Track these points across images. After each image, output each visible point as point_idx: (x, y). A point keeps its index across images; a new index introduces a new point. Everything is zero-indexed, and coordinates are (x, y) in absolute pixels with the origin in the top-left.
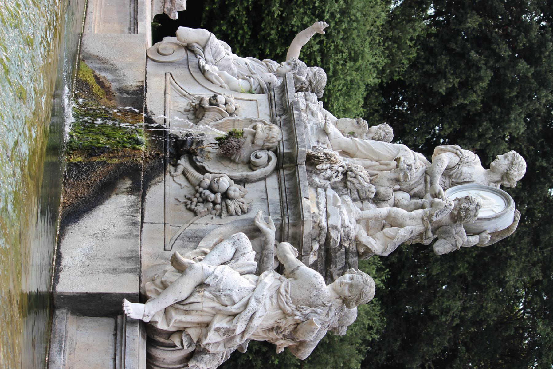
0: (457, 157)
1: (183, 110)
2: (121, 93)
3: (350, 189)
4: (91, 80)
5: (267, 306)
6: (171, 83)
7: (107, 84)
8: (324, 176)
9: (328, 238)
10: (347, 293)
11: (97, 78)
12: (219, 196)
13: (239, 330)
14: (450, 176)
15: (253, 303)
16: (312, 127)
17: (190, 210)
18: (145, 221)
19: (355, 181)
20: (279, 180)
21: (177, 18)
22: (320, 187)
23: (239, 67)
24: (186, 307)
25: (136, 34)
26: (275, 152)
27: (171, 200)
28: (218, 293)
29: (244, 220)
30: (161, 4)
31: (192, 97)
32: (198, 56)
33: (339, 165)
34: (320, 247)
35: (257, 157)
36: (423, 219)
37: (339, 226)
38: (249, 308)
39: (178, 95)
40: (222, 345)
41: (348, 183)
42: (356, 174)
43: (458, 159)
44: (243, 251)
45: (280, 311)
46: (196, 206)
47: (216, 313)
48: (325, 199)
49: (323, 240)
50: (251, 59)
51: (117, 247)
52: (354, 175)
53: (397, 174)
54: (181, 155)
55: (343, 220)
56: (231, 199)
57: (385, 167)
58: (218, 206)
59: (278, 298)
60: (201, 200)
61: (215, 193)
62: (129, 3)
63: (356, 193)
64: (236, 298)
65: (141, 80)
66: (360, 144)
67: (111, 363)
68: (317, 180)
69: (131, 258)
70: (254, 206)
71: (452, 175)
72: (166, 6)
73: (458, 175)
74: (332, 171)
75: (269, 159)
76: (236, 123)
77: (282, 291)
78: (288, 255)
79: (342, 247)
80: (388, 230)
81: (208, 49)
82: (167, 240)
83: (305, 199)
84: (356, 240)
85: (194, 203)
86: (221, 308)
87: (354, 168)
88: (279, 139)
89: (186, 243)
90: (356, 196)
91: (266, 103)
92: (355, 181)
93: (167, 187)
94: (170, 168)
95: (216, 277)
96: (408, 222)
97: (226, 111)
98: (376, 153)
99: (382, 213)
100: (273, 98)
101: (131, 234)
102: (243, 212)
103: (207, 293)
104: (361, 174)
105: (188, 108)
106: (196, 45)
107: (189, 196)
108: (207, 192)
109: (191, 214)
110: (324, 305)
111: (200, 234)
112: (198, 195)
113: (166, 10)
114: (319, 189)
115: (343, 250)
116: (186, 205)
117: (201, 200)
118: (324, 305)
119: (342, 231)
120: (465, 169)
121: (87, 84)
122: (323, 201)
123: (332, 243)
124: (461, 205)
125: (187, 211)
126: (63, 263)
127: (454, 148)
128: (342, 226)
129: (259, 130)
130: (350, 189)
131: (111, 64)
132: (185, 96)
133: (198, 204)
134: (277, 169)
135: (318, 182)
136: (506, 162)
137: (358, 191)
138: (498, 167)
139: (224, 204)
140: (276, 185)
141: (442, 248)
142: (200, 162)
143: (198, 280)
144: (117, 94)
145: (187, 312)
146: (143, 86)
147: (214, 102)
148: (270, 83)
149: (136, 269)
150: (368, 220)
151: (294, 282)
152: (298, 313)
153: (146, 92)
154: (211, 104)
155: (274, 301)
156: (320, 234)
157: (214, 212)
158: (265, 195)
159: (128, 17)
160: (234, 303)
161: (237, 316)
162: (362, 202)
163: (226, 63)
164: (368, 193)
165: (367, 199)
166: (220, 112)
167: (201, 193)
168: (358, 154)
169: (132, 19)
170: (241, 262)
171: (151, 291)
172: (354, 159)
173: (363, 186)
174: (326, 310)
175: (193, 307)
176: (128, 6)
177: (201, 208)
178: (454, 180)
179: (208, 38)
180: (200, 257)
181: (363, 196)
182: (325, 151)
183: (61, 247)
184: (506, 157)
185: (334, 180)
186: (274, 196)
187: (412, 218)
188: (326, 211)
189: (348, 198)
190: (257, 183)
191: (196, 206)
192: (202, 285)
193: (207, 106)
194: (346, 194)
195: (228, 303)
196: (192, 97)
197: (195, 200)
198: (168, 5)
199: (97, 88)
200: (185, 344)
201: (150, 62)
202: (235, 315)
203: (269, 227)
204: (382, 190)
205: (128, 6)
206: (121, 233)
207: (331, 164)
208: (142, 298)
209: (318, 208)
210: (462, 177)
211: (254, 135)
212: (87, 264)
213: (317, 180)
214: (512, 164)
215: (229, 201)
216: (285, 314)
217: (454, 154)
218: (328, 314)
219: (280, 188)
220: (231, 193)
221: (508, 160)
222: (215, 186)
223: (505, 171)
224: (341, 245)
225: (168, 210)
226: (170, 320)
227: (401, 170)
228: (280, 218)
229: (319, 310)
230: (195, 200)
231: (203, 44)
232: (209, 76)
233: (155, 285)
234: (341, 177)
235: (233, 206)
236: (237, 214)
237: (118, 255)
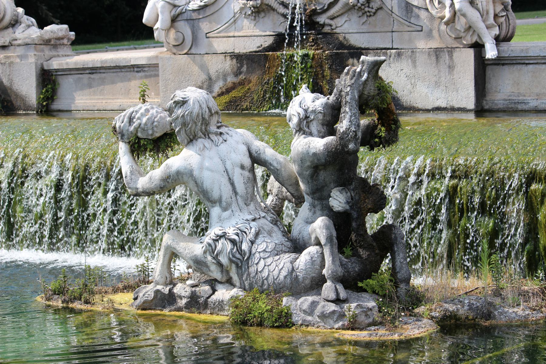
2: (240, 73)
4: (226, 98)
6: (218, 33)
7: (230, 85)
11: (221, 94)
17: (375, 13)
18: (391, 47)
21: (73, 33)
24: (485, 14)
25: (160, 66)
27: (365, 28)
30: (65, 48)
32: (184, 11)
39: (234, 27)
46: (372, 8)
51: (425, 67)
54: (313, 21)
62: (99, 75)
65: (224, 58)
67: (531, 66)
69: (437, 55)
72: (66, 43)
85: (370, 10)
89: (414, 14)
93: (350, 31)
94: (327, 29)
101: (411, 57)
105: (253, 18)
107: (360, 14)
109: (380, 12)
111: (403, 5)
112: (363, 7)
113: (69, 43)
116: (370, 16)
117: (367, 5)
121: (230, 102)
126: (443, 105)
131: (203, 83)
133: (371, 6)
142: (324, 6)
144: (242, 77)
145: (488, 13)
146: (231, 56)
149: (448, 52)
153: (233, 52)
159: (119, 74)
167: (362, 5)
169: (123, 70)
171: (472, 40)
175: (485, 8)
176: (103, 75)
183: (427, 108)
191: (372, 8)
197: (367, 9)
198: (65, 41)
199: (234, 94)
201: (193, 51)
205: (103, 75)
206: (410, 64)
212: (445, 88)
225: (378, 30)
226: (493, 25)
230: (367, 9)
231: (171, 7)
237: (434, 65)
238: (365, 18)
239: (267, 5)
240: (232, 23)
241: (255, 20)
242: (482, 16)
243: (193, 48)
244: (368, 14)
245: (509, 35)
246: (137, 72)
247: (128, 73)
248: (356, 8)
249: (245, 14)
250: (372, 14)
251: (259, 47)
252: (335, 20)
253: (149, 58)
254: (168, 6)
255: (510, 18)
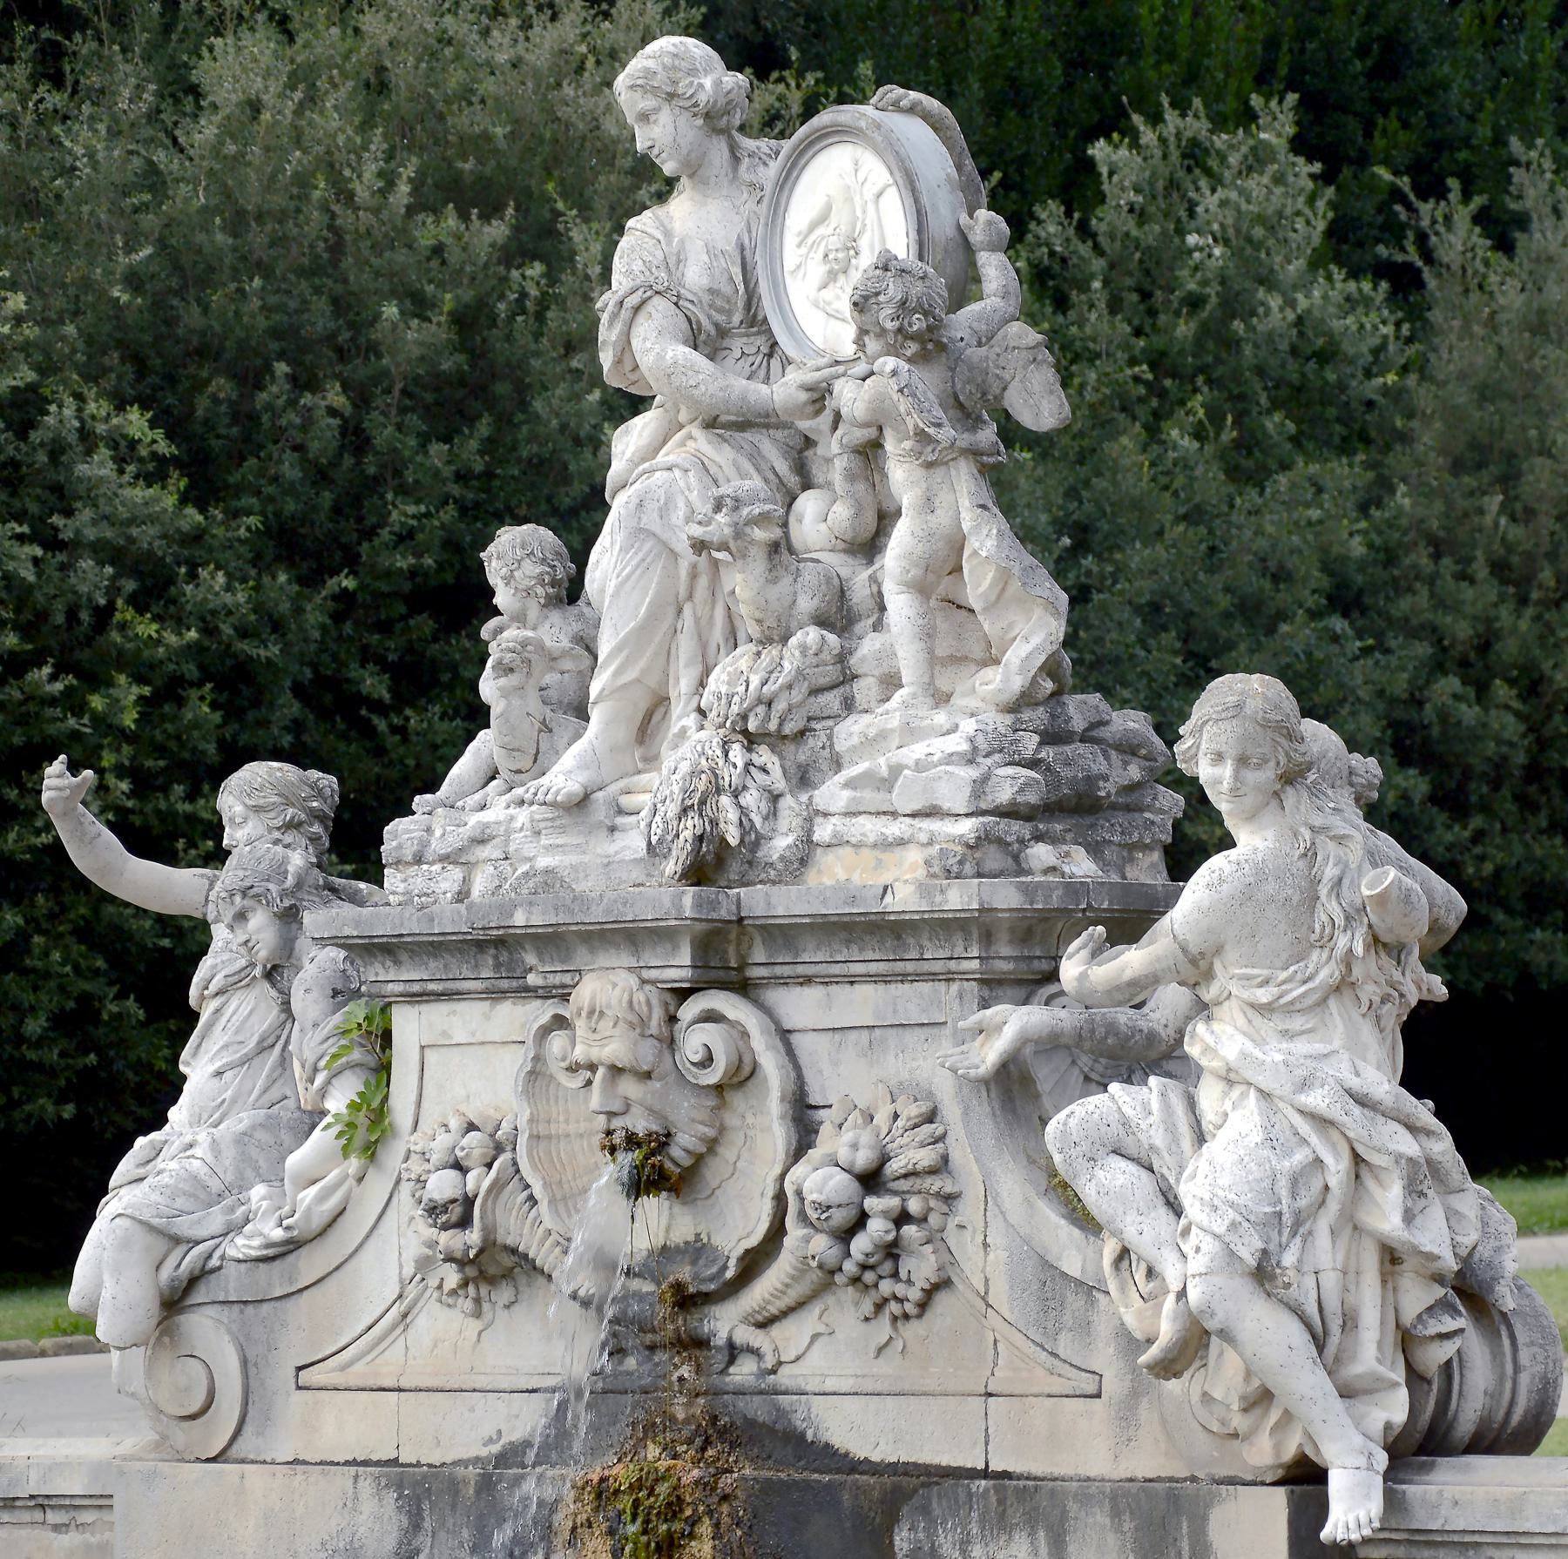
0: (649, 307)
1: (474, 1326)
3: (809, 719)
5: (1320, 1048)
6: (343, 1368)
8: (766, 818)
9: (1009, 812)
10: (1268, 774)
12: (871, 1203)
13: (1408, 1145)
14: (722, 332)
15: (1316, 1099)
16: (551, 849)
17: (923, 1306)
18: (981, 1466)
19: (780, 706)
20: (784, 982)
22: (809, 832)
23: (234, 1101)
25: (115, 1502)
26: (683, 995)
27: (887, 1370)
28: (1287, 1219)
29: (966, 1113)
31: (412, 1292)
32: (215, 1262)
33: (721, 762)
34: (1039, 838)
35: (708, 1061)
36: (929, 465)
37: (972, 773)
38: (1336, 1113)
39: (401, 1340)
40: (1457, 1202)
41: (789, 729)
42: (759, 701)
43: (657, 300)
44: (1117, 1128)
45: (1332, 1003)
46: (909, 1282)
47: (1351, 1226)
48: (861, 819)
49: (1016, 829)
50: (195, 1054)
52: (761, 709)
53: (753, 551)
55: (949, 759)
56: (884, 1159)
57: (703, 582)
58: (914, 1206)
59: (1290, 1009)
60: (887, 1267)
61: (862, 1219)
63: (823, 699)
64: (1300, 1157)
66: (617, 674)
68: (781, 844)
70: (905, 1076)
71: (717, 325)
73: (719, 303)
74: (745, 788)
75: (711, 1017)
76: (542, 1129)
77: (1263, 995)
78: (1128, 975)
79: (1040, 761)
80: (977, 586)
81: (183, 1226)
82: (1058, 1386)
83: (888, 898)
84: (1014, 708)
85: (900, 1289)
86: (1333, 1206)
87: (735, 709)
88: (633, 981)
89: (1068, 1319)
90: (832, 700)
91: (436, 1015)
92: (780, 706)
93: (830, 1385)
95: (1234, 1226)
96: (942, 518)
97: (489, 1166)
98: (652, 617)
99: (911, 612)
100: (416, 988)
102: (931, 1117)
103: (1289, 1259)
104: (755, 681)
105: (468, 1305)
106: (166, 1273)
107: (867, 1307)
108: (861, 1244)
109: (942, 1300)
110: (1310, 854)
112: (869, 1277)
114: (816, 838)
115: (1048, 753)
116: (906, 1317)
118: (1310, 854)
119: (989, 761)
120: (695, 276)
122: (869, 827)
123: (1032, 798)
124: (884, 331)
125: (929, 1315)
127: (614, 317)
128: (971, 762)
129: (596, 1054)
130: (809, 719)
132: (405, 1316)
133: (903, 1274)
134: (743, 987)
135: (790, 840)
136: (665, 117)
137: (815, 691)
138: (684, 151)
139: (903, 1185)
140: (814, 993)
141: (1040, 403)
142: (725, 1268)
143: (1243, 1289)
145: (1350, 1322)
147: (456, 1212)
148: (335, 993)
150: (934, 662)
151: (1231, 954)
152: (1342, 942)
153: (394, 1462)
154: (464, 1222)
155: (1297, 1023)
156: (1001, 842)
157: (934, 1220)
158: (853, 1035)
160: (1318, 1162)
161: (1361, 1150)
162: (855, 677)
163: (229, 1154)
164: (825, 656)
165: (842, 658)
166: (497, 1187)
167: (864, 1267)
168: (652, 681)
170: (1159, 1139)
171: (1277, 1447)
172: (673, 694)
173: (800, 674)
174: (1327, 848)
175: (1333, 1305)
177: (921, 1267)
178: (737, 319)
179: (138, 1228)
180: (1140, 1276)
181: (830, 673)
182: (673, 809)
184: (644, 117)
185: (777, 780)
186: (861, 1003)
187: (928, 504)
188: (913, 815)
189: (850, 731)
190: (804, 1061)
192: (1263, 1274)
193: (474, 1236)
194: (830, 737)
195: (1317, 1185)
196: (412, 1292)
197: (886, 1287)
200: (1449, 1324)
201: (242, 1448)
202: (1357, 1159)
203: (999, 1028)
204: (806, 604)
207: (719, 791)
208: (1306, 1479)
209: (901, 842)
210: (727, 289)
211: (616, 1071)
213: (781, 844)
214: (671, 96)
215: (894, 1167)
216: (1344, 986)
217: (641, 318)
218: (1340, 840)
219: (828, 981)
220: (863, 1159)
221: (657, 110)
222: (840, 1217)
223: (700, 122)
224: (1033, 764)
225: (930, 1384)
226: (1379, 1379)
227: (738, 535)
228: (955, 987)
229: (1330, 872)
230: (886, 1287)
231: (161, 1245)
232: (317, 1223)
233: (1253, 1431)
234: (764, 756)
235: (910, 1155)
236: (941, 1138)
238: (883, 1328)
239: (514, 1251)
240: (394, 1327)
241: (478, 1314)
242: (1319, 1342)
243: (248, 1429)
244: (894, 1307)
245: (1516, 1418)
246: (57, 1528)
247: (23, 1532)
248: (838, 1278)
249: (440, 1287)
250: (909, 1308)
251: (491, 1441)
252: (776, 1331)
253: (99, 1469)
254: (141, 1238)
255: (1522, 1338)
